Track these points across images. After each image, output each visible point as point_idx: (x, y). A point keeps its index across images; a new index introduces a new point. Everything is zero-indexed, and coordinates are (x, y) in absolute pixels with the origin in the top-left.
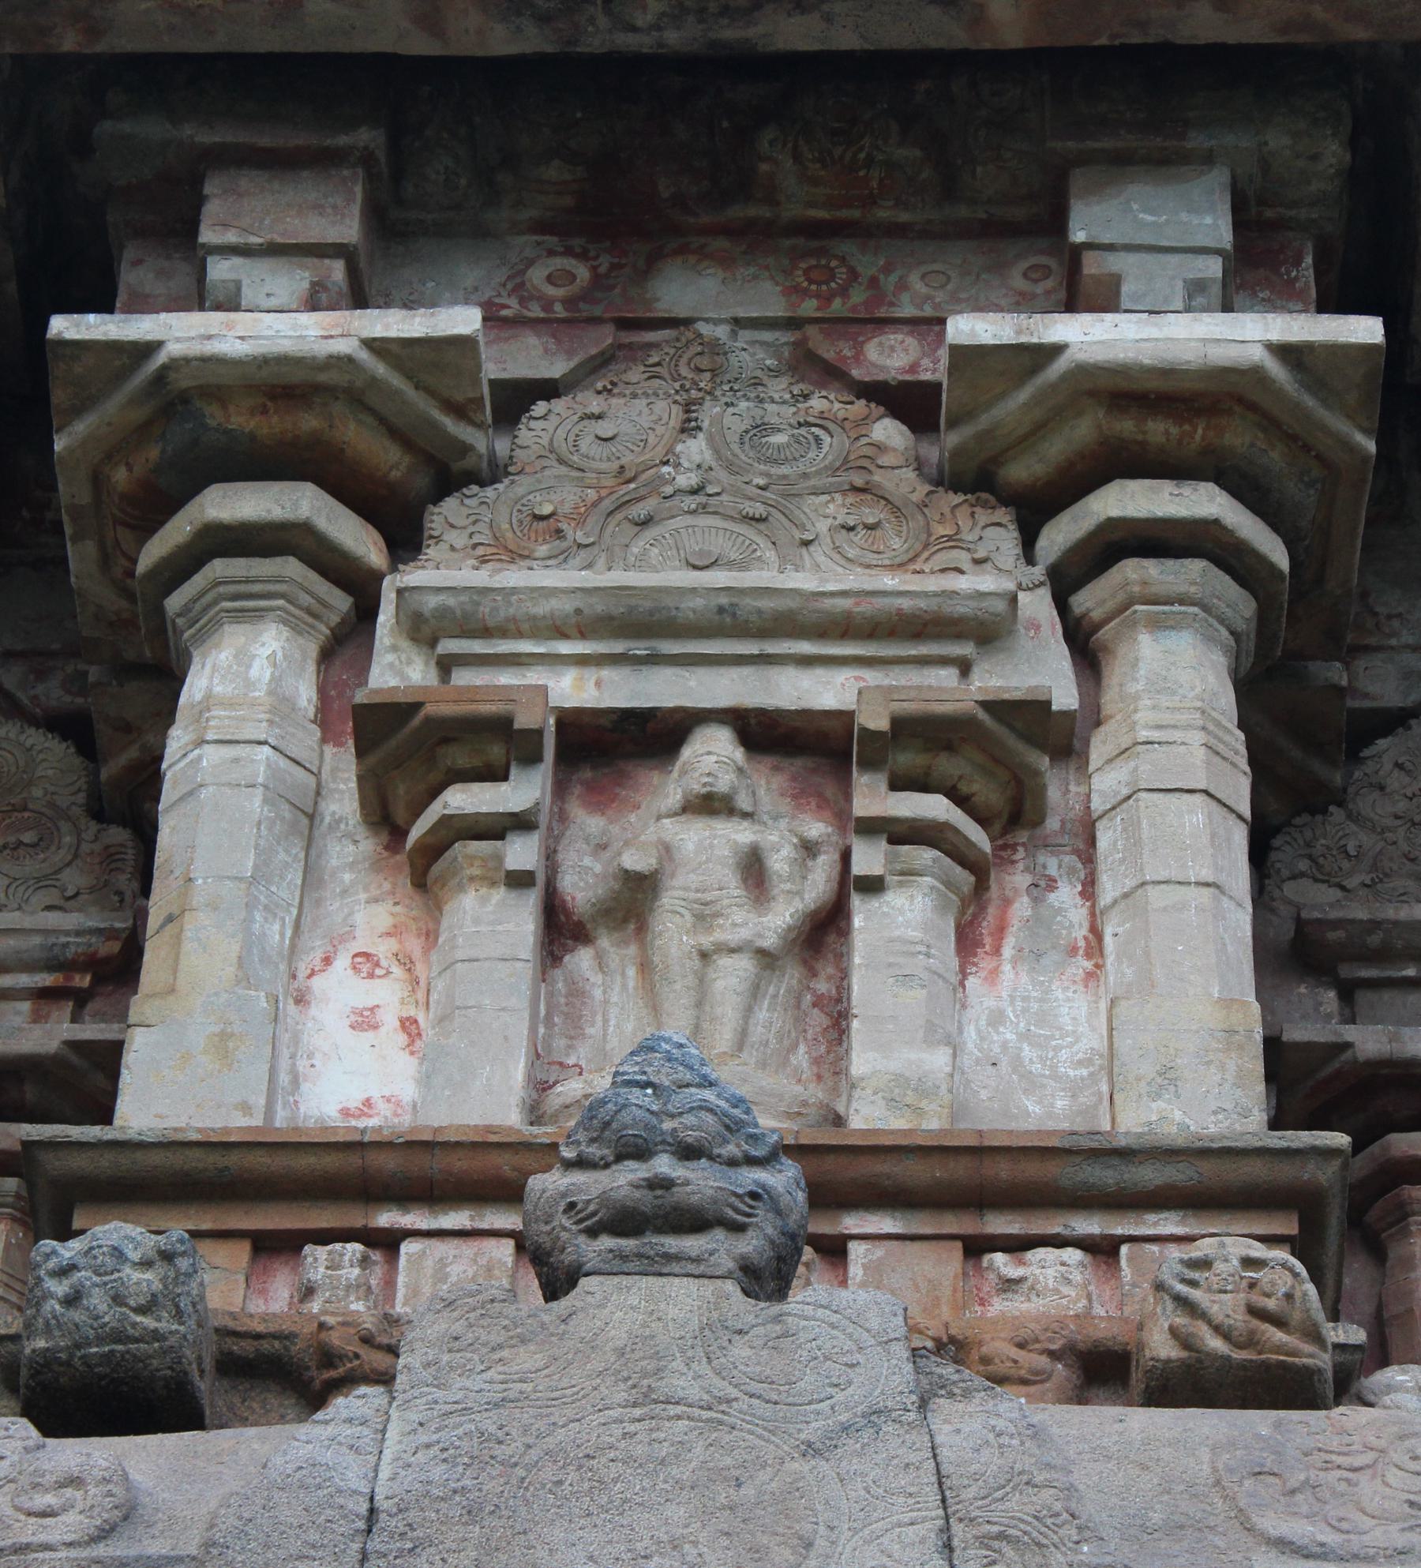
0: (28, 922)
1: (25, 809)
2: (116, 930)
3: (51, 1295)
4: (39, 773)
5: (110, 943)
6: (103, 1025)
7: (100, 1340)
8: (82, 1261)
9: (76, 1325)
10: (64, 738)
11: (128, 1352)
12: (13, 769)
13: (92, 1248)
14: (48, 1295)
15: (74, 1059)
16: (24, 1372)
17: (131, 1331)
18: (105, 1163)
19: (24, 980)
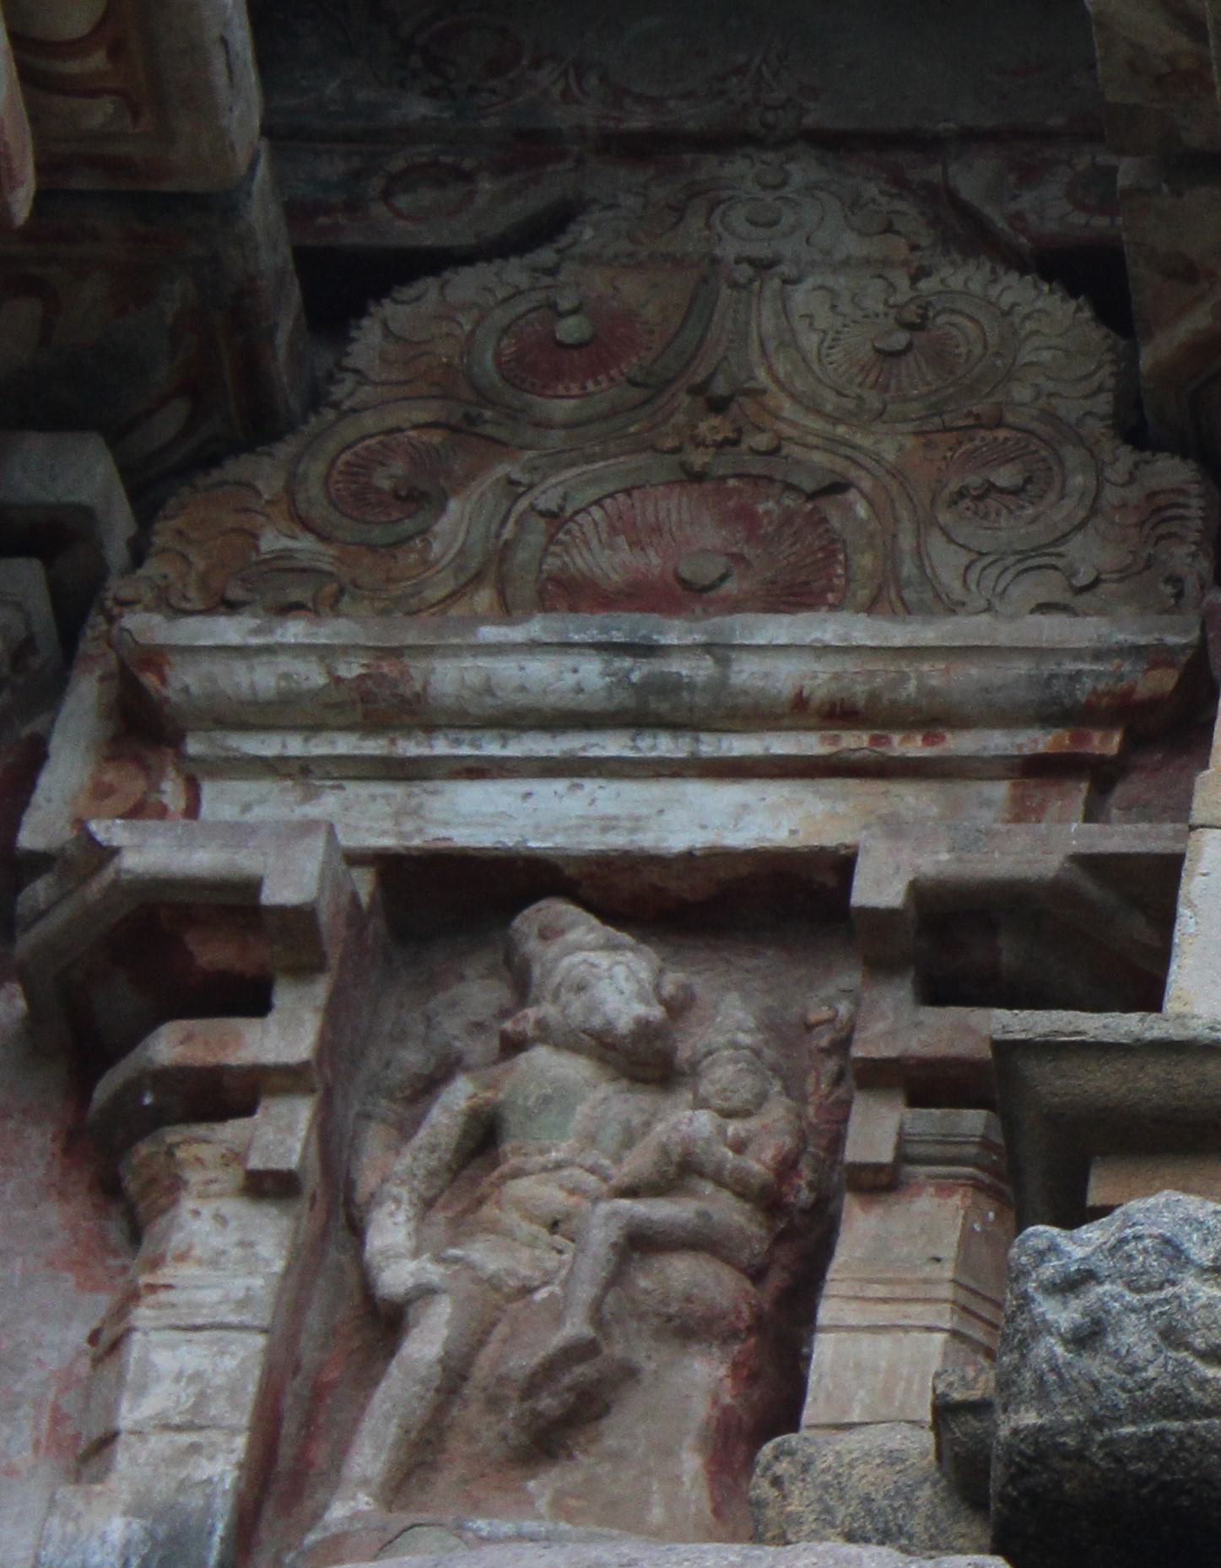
0: (1005, 634)
1: (999, 423)
2: (1171, 650)
3: (1048, 1328)
4: (1025, 356)
5: (1157, 673)
6: (1144, 826)
7: (1139, 1412)
8: (1104, 1265)
9: (1095, 1384)
10: (1073, 292)
11: (1190, 1434)
12: (978, 350)
13: (1123, 1241)
14: (1043, 1328)
15: (1090, 888)
16: (997, 1471)
17: (1196, 1395)
18: (1148, 1083)
19: (998, 742)
